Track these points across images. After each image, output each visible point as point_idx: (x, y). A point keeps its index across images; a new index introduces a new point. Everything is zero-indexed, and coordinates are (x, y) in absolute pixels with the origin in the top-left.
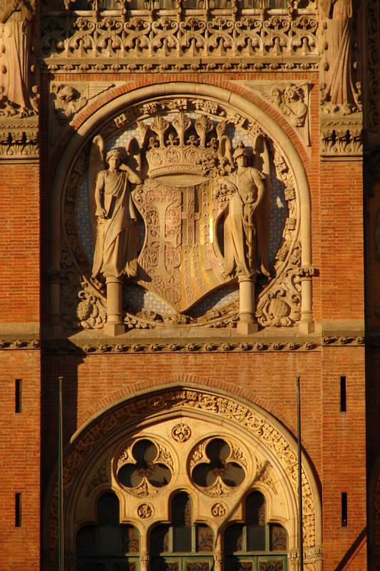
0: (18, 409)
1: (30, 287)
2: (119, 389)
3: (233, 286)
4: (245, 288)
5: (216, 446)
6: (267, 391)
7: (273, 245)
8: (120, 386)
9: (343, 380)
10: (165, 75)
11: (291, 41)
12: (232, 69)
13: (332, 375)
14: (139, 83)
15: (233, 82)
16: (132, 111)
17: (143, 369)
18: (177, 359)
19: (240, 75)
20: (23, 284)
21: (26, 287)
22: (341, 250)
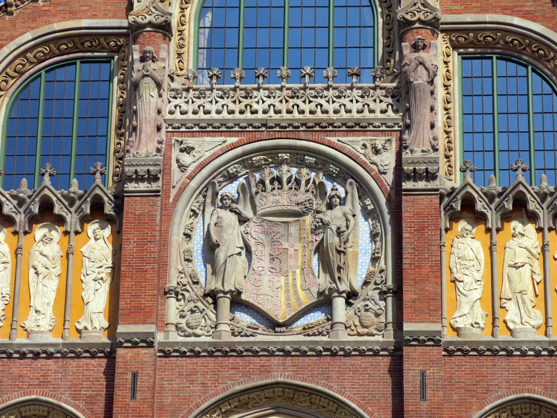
0: (133, 397)
1: (149, 295)
2: (225, 385)
6: (355, 388)
7: (361, 271)
8: (224, 383)
9: (423, 374)
10: (271, 133)
11: (378, 107)
13: (413, 370)
14: (249, 139)
15: (329, 138)
17: (246, 369)
18: (274, 361)
19: (333, 133)
20: (143, 293)
21: (145, 295)
22: (420, 266)
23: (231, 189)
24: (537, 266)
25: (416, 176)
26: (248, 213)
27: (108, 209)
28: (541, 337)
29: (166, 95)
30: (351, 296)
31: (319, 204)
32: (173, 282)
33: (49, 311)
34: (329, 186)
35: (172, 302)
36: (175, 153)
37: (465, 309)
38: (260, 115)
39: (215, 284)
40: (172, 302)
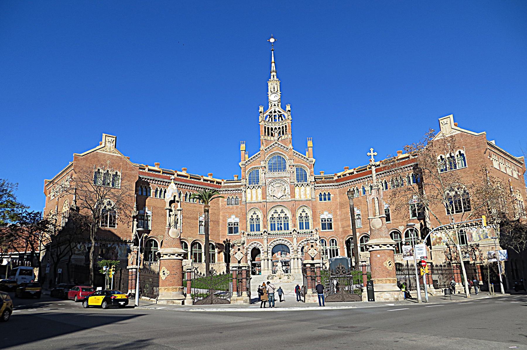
3: (283, 196)
4: (284, 196)
5: (282, 210)
12: (282, 177)
16: (273, 181)
23: (272, 184)
24: (304, 191)
28: (305, 199)
30: (285, 195)
36: (267, 180)
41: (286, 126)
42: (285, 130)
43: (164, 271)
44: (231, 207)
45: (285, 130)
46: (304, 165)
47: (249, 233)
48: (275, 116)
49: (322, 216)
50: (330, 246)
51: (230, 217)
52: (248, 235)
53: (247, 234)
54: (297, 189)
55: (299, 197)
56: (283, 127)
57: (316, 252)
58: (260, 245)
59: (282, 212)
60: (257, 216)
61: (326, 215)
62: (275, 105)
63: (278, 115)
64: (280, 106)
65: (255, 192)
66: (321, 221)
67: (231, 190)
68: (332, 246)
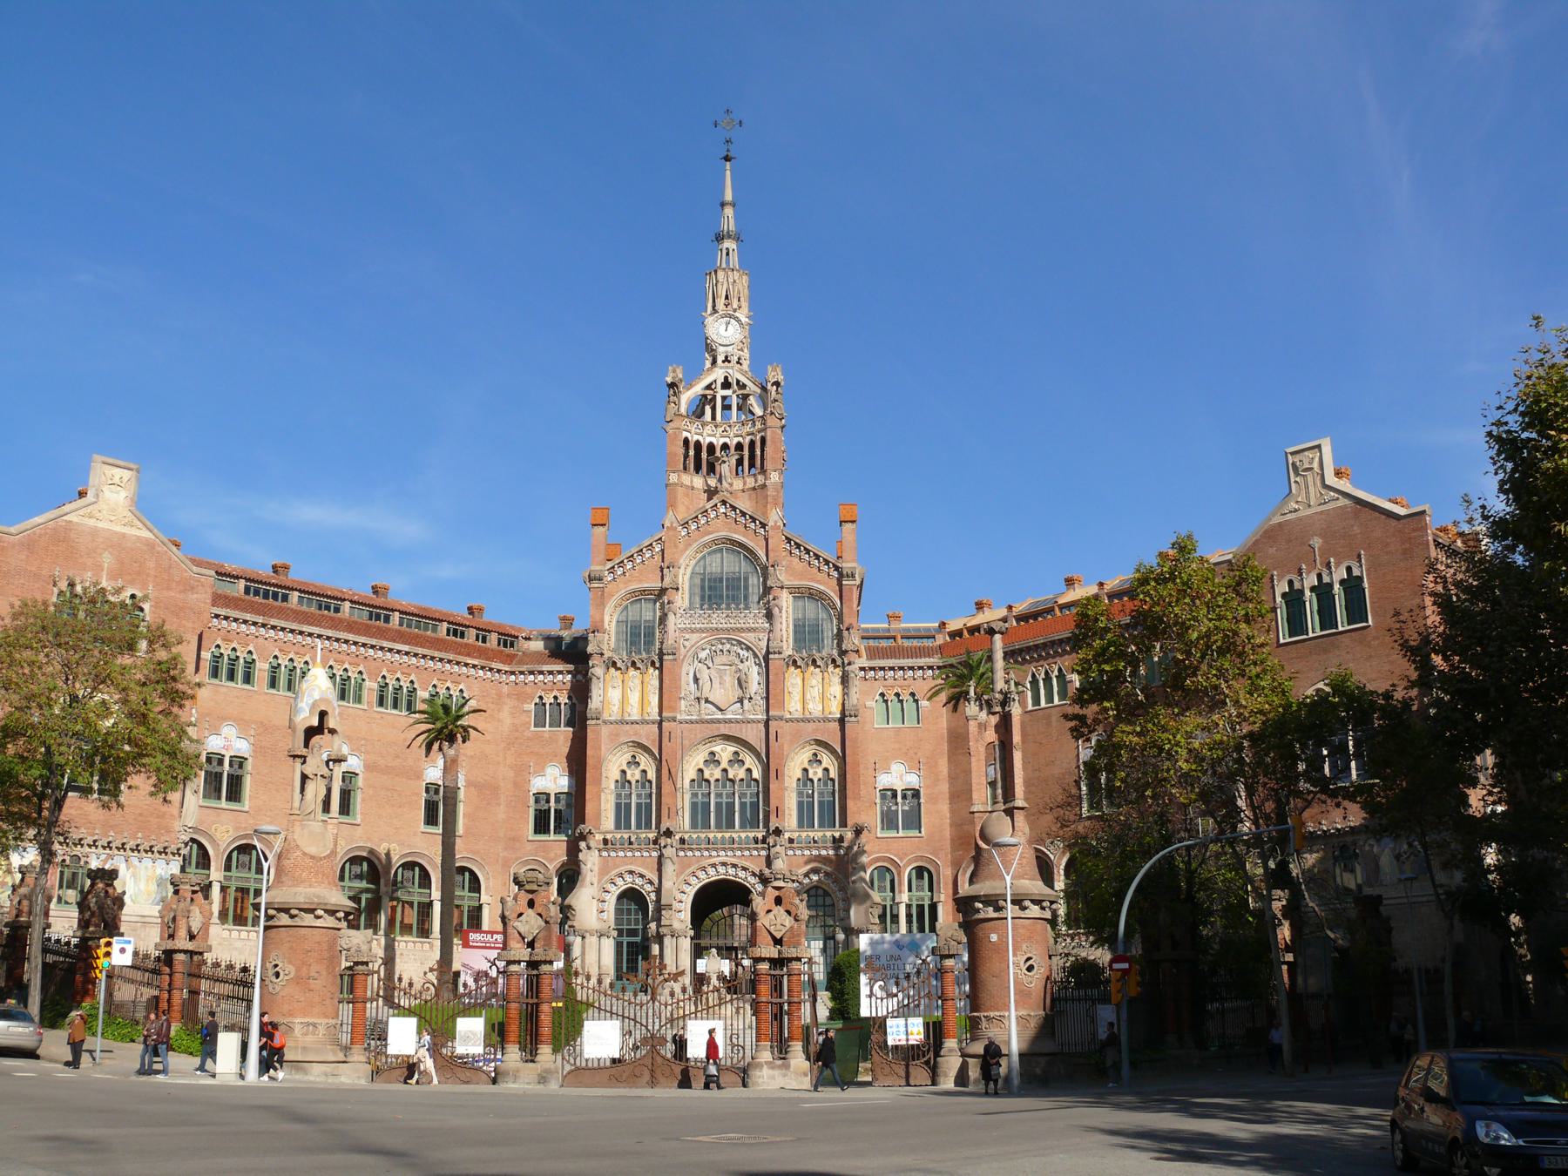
5: (736, 753)
11: (760, 621)
12: (739, 630)
18: (722, 725)
23: (703, 655)
25: (775, 653)
26: (710, 665)
27: (657, 665)
29: (679, 615)
31: (737, 661)
32: (682, 695)
33: (636, 705)
34: (741, 652)
35: (683, 702)
37: (793, 704)
38: (715, 626)
39: (699, 695)
40: (683, 702)
41: (763, 440)
42: (758, 452)
43: (276, 966)
44: (546, 735)
45: (758, 452)
46: (822, 587)
47: (609, 837)
48: (724, 398)
49: (884, 781)
50: (910, 890)
51: (540, 772)
52: (605, 841)
53: (599, 837)
54: (793, 678)
55: (799, 707)
56: (752, 443)
57: (788, 921)
58: (651, 883)
59: (736, 760)
60: (644, 771)
61: (898, 776)
62: (727, 360)
63: (738, 396)
64: (746, 365)
65: (637, 682)
66: (878, 801)
67: (551, 673)
68: (917, 890)
